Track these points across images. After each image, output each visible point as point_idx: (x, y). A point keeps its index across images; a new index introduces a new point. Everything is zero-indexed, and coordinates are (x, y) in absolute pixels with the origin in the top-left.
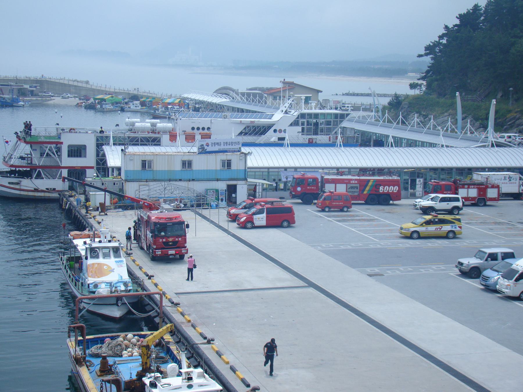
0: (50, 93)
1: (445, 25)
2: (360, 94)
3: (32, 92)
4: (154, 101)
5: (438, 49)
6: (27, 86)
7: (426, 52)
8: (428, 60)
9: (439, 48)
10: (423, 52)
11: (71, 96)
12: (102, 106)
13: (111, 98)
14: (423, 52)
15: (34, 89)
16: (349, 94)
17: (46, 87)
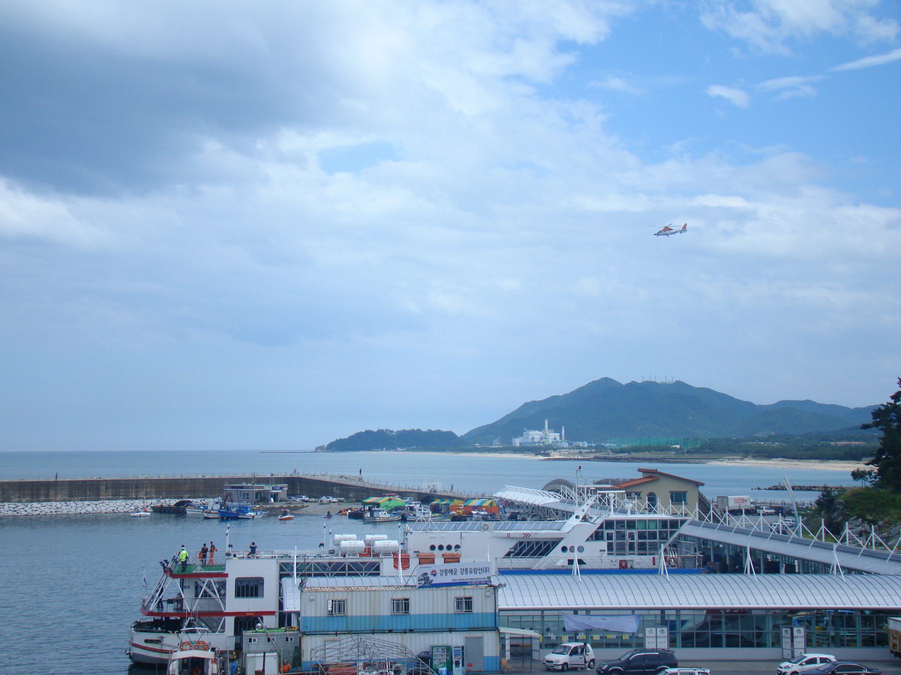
0: (304, 497)
1: (899, 378)
2: (797, 487)
3: (275, 496)
4: (452, 504)
5: (894, 416)
6: (267, 488)
7: (875, 420)
8: (878, 433)
9: (896, 413)
10: (870, 420)
11: (334, 501)
12: (372, 515)
13: (388, 503)
14: (870, 420)
15: (280, 491)
16: (779, 488)
17: (299, 488)
